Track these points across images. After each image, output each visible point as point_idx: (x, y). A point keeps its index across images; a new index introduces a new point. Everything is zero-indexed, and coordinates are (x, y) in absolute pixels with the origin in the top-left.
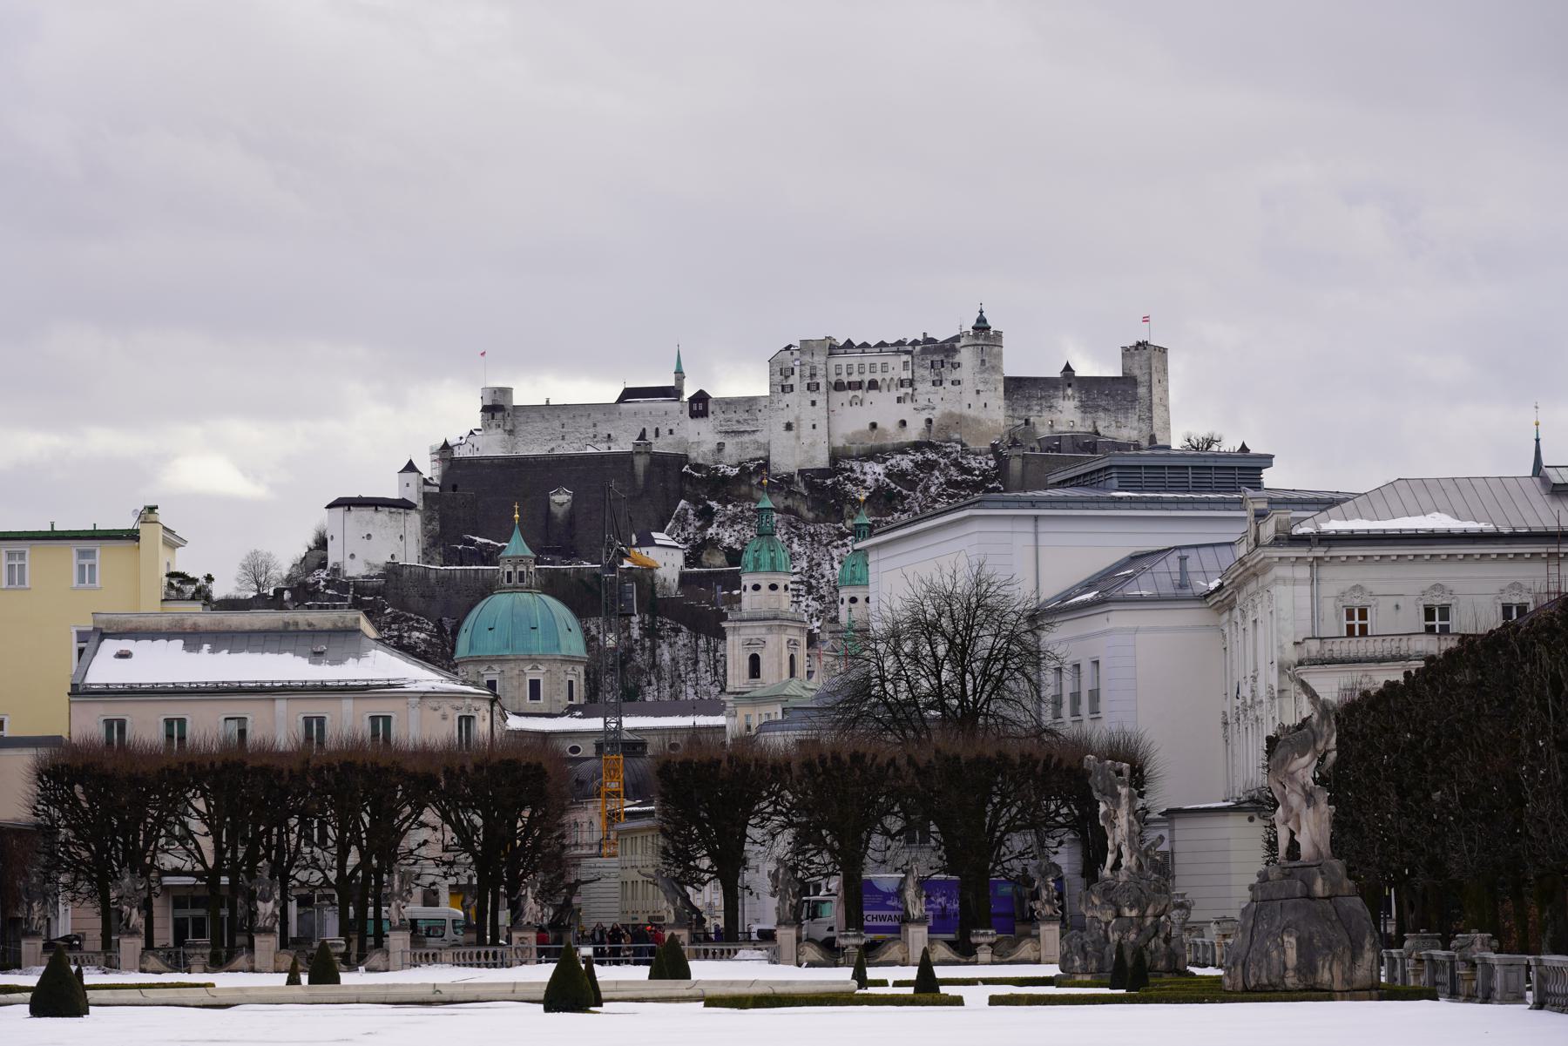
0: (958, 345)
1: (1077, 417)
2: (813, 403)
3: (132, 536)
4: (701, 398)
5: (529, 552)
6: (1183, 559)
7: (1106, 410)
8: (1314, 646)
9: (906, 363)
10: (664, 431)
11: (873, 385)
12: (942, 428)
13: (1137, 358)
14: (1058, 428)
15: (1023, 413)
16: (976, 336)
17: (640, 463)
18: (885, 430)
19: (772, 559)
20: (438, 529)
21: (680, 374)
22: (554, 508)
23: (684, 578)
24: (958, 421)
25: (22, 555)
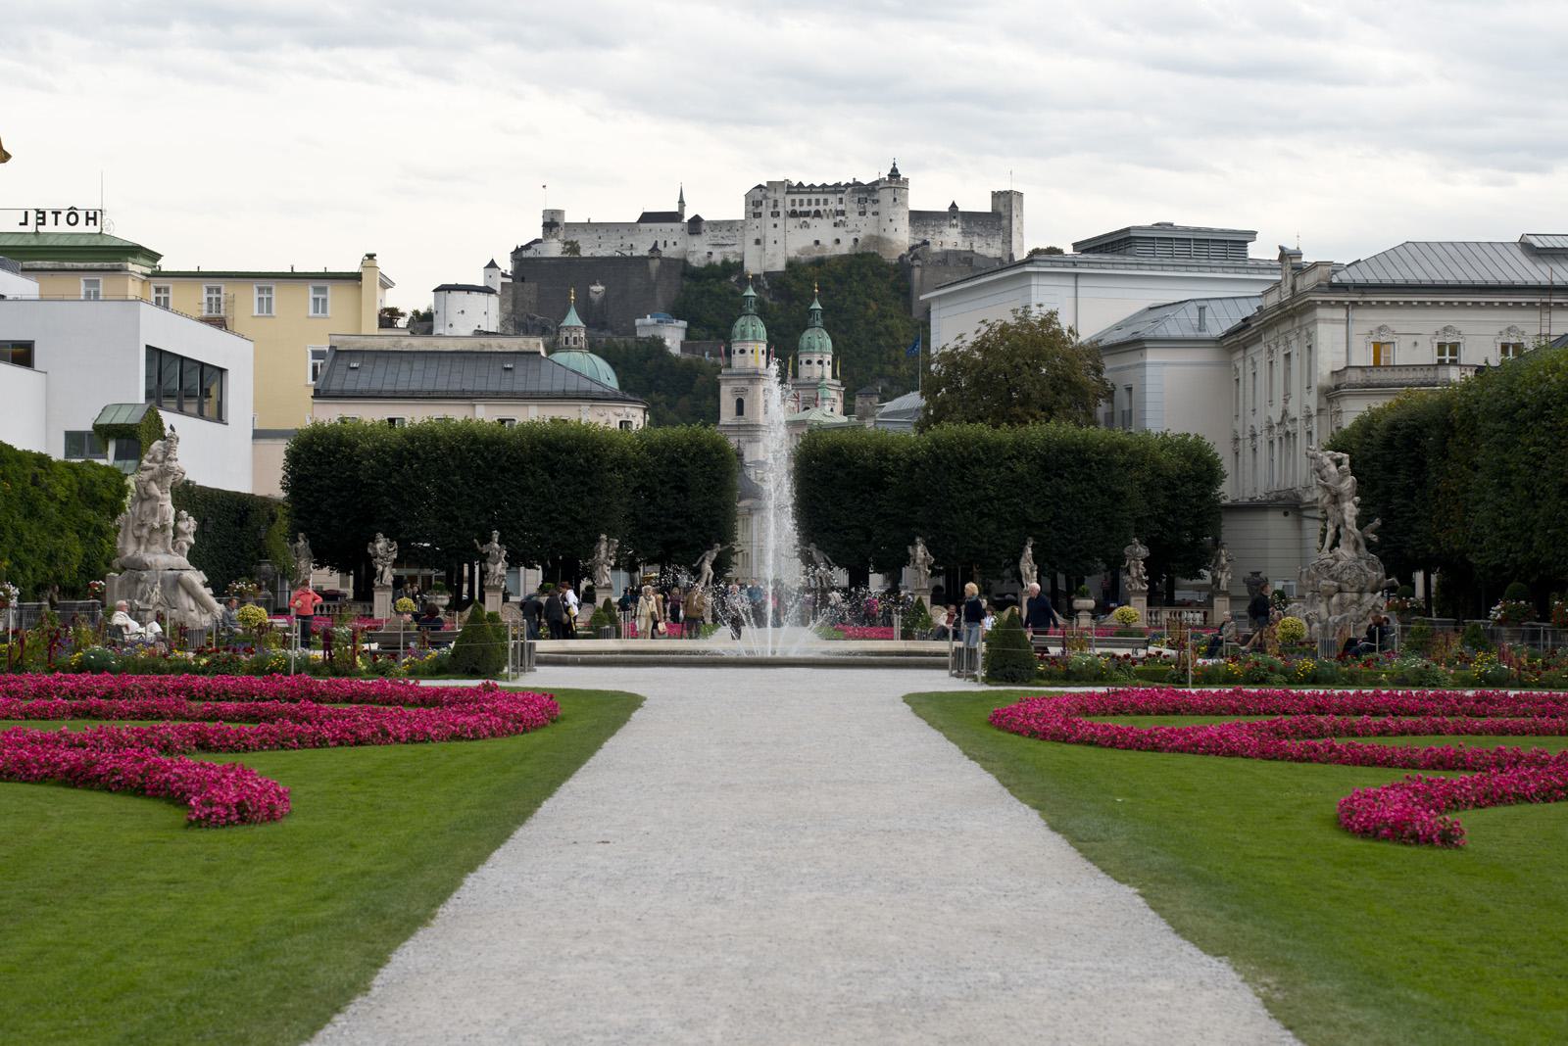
0: (877, 187)
1: (959, 239)
2: (775, 226)
3: (356, 277)
4: (696, 220)
5: (581, 324)
6: (1201, 309)
8: (1355, 377)
10: (670, 243)
11: (818, 214)
13: (1002, 199)
14: (947, 247)
15: (922, 236)
16: (890, 181)
17: (655, 264)
18: (824, 246)
20: (511, 308)
21: (681, 202)
22: (592, 295)
23: (684, 347)
24: (877, 240)
25: (270, 290)
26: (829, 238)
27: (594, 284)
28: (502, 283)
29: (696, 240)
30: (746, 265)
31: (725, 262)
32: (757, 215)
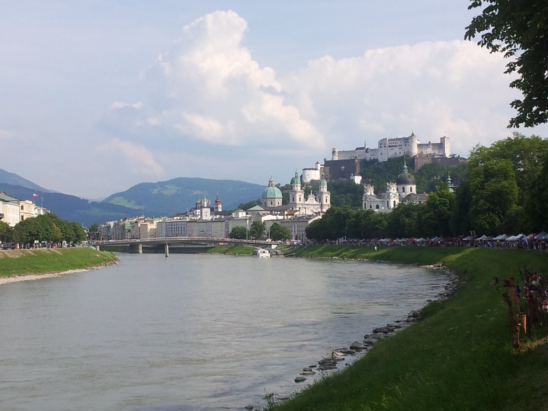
1: (431, 151)
2: (385, 150)
7: (437, 149)
9: (400, 142)
10: (362, 155)
11: (395, 146)
12: (406, 153)
14: (427, 153)
15: (421, 150)
19: (296, 182)
21: (365, 145)
22: (342, 169)
23: (361, 181)
26: (397, 152)
27: (342, 166)
28: (321, 168)
29: (367, 153)
30: (379, 160)
31: (374, 159)
32: (381, 147)
